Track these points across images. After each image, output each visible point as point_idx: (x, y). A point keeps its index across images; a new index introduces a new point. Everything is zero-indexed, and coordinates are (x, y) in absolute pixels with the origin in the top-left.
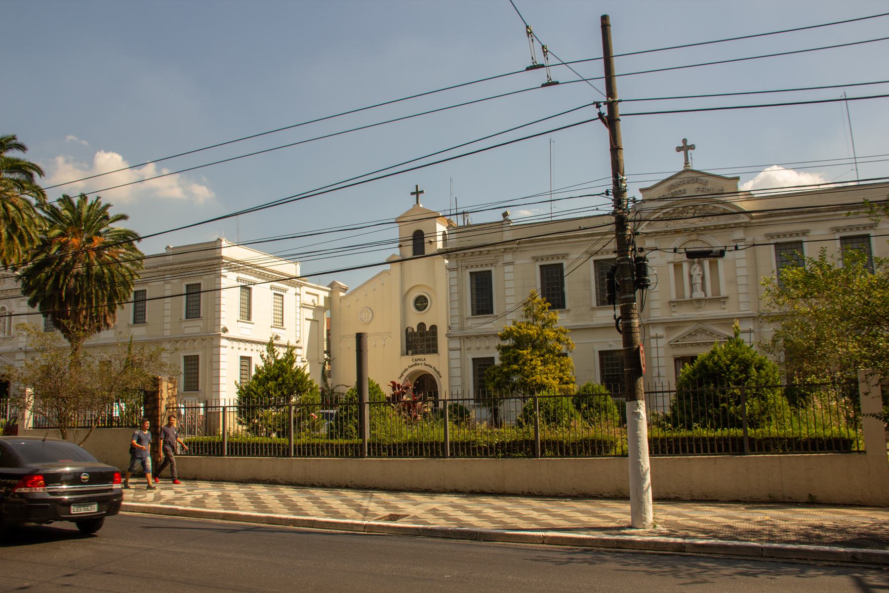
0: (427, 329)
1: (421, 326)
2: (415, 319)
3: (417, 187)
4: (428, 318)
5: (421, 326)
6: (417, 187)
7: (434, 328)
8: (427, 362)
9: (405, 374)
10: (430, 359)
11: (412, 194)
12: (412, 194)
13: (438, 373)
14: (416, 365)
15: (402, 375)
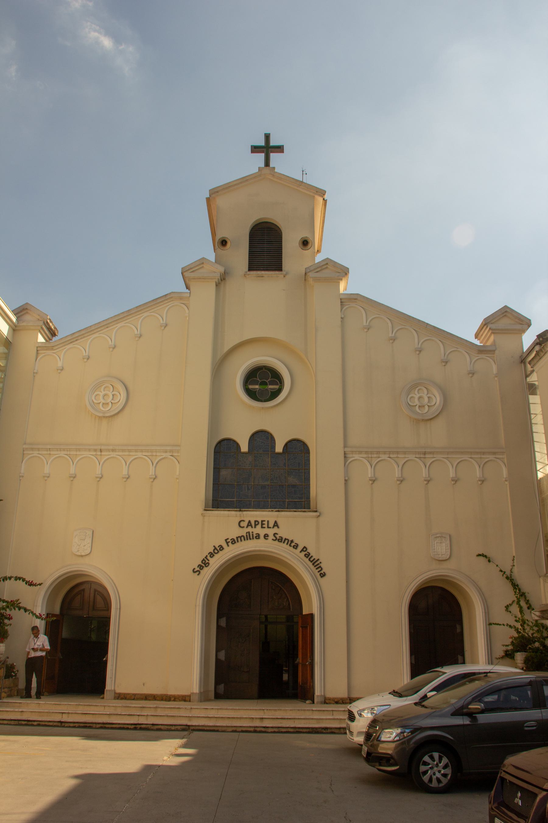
0: (279, 448)
1: (262, 438)
2: (244, 421)
3: (267, 137)
4: (282, 422)
5: (262, 438)
6: (267, 137)
7: (298, 450)
8: (282, 532)
9: (216, 563)
10: (291, 523)
11: (255, 149)
12: (255, 149)
13: (316, 563)
14: (249, 537)
15: (205, 563)
